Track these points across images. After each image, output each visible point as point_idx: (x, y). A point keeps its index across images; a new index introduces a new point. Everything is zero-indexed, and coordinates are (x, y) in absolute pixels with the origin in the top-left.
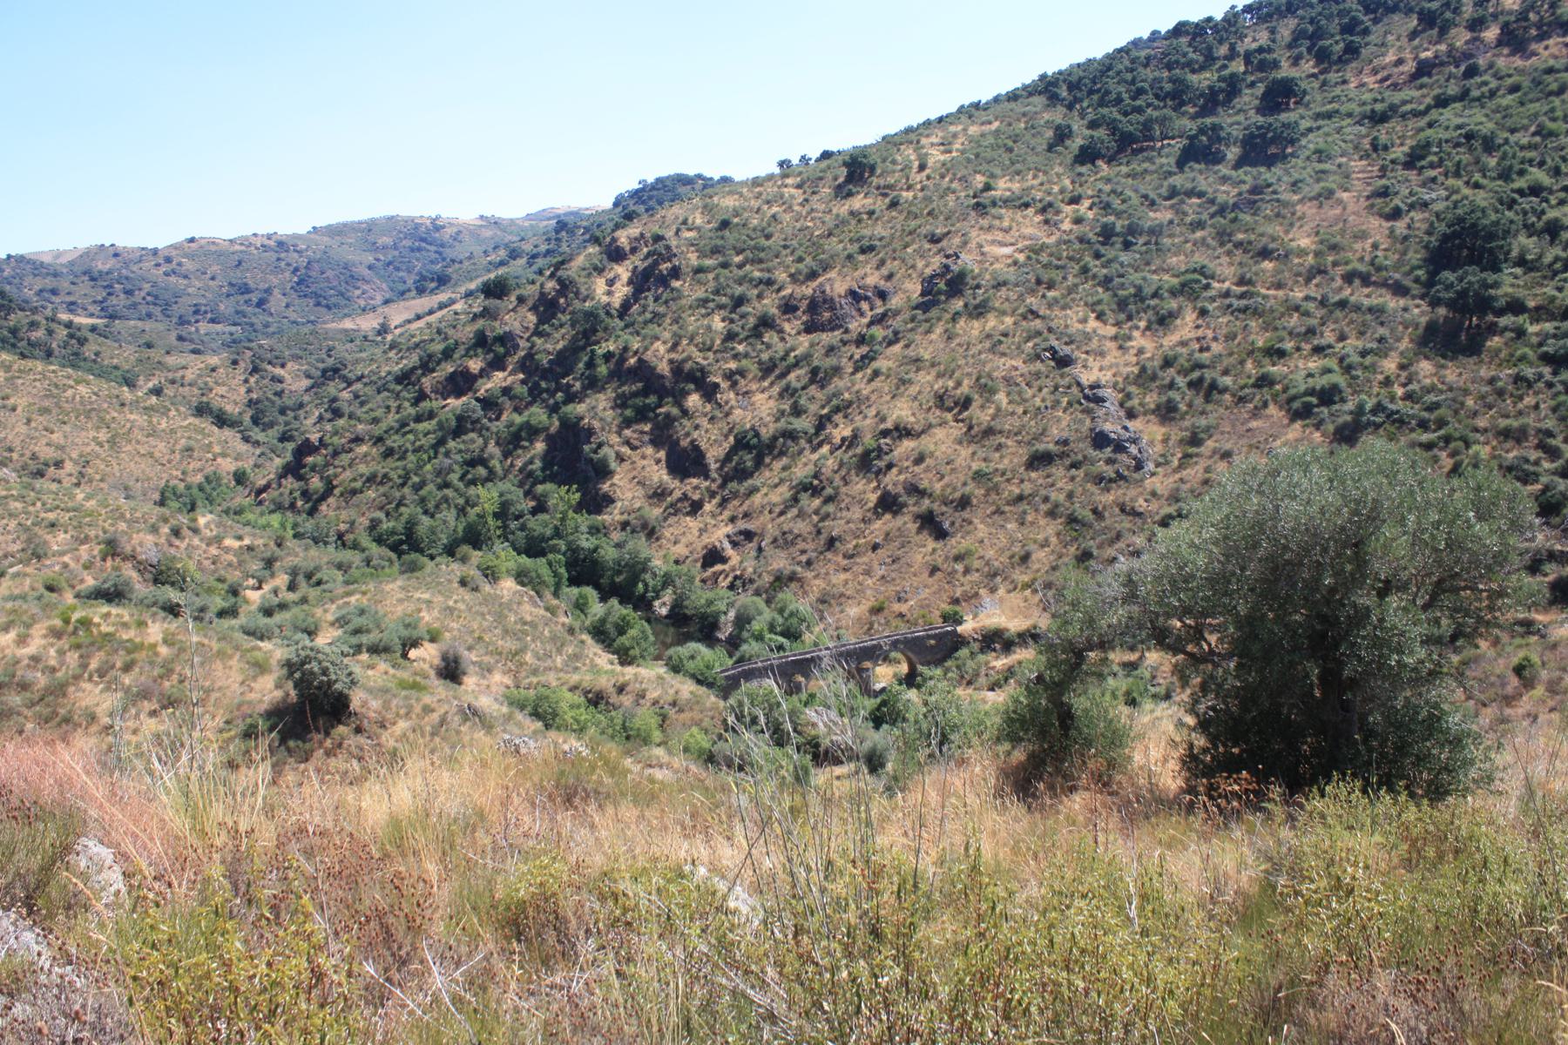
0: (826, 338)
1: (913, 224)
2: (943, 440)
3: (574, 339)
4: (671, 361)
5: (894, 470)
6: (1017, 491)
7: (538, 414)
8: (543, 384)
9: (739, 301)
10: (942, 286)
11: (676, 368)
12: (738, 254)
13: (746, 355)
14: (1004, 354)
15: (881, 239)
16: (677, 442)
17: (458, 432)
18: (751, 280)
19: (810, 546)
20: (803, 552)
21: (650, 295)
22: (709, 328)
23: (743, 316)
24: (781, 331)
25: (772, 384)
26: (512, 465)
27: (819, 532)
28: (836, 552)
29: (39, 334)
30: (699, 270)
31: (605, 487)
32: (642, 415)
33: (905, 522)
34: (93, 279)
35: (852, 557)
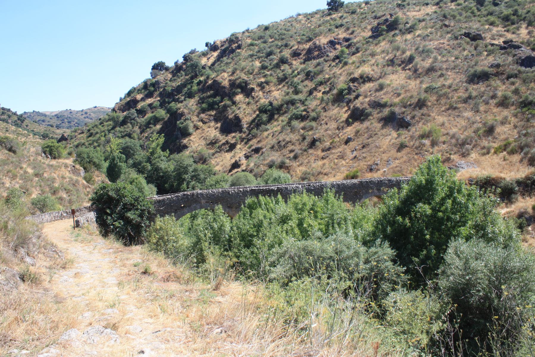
0: (315, 62)
1: (364, 16)
2: (397, 79)
3: (187, 80)
4: (230, 80)
5: (361, 98)
6: (466, 95)
7: (162, 113)
8: (167, 100)
9: (270, 54)
10: (384, 27)
11: (233, 84)
12: (271, 38)
13: (271, 75)
14: (431, 40)
15: (347, 23)
16: (228, 118)
17: (124, 123)
18: (277, 45)
19: (297, 148)
20: (292, 151)
21: (225, 58)
22: (253, 65)
23: (270, 61)
24: (291, 64)
25: (284, 86)
26: (143, 136)
27: (304, 139)
28: (316, 149)
29: (5, 117)
30: (252, 45)
31: (185, 141)
32: (211, 107)
33: (373, 123)
34: (58, 118)
35: (329, 149)
